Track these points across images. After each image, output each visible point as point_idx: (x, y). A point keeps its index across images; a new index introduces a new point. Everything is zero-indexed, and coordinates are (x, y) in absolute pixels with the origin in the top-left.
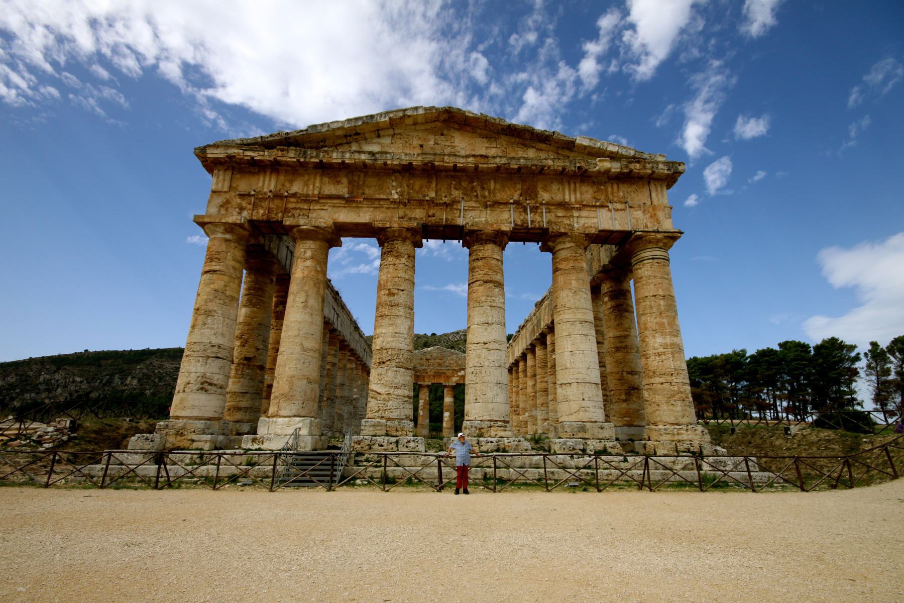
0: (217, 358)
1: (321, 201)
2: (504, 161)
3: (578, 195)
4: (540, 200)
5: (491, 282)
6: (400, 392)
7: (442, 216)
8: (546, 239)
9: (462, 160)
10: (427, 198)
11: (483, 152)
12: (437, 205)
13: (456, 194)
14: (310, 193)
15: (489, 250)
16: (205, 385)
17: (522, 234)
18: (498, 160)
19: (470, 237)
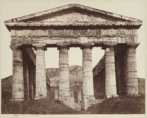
0: (21, 83)
1: (41, 38)
2: (92, 23)
3: (113, 33)
4: (102, 35)
5: (89, 60)
6: (67, 90)
7: (74, 40)
8: (104, 46)
9: (80, 24)
10: (71, 36)
11: (85, 20)
12: (74, 38)
13: (79, 34)
14: (38, 35)
15: (88, 50)
16: (20, 90)
17: (97, 45)
18: (90, 23)
19: (83, 47)
